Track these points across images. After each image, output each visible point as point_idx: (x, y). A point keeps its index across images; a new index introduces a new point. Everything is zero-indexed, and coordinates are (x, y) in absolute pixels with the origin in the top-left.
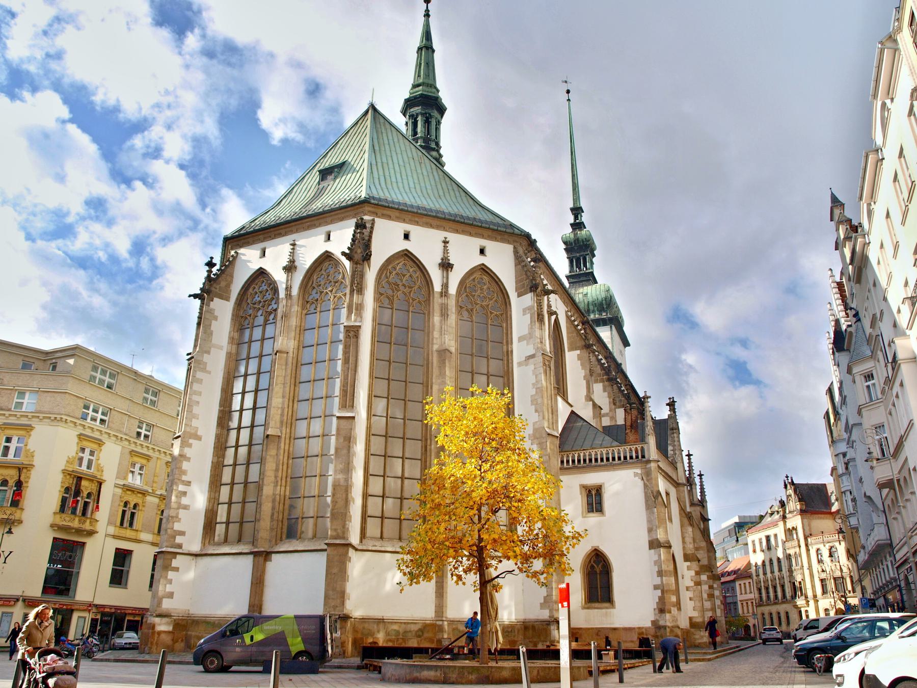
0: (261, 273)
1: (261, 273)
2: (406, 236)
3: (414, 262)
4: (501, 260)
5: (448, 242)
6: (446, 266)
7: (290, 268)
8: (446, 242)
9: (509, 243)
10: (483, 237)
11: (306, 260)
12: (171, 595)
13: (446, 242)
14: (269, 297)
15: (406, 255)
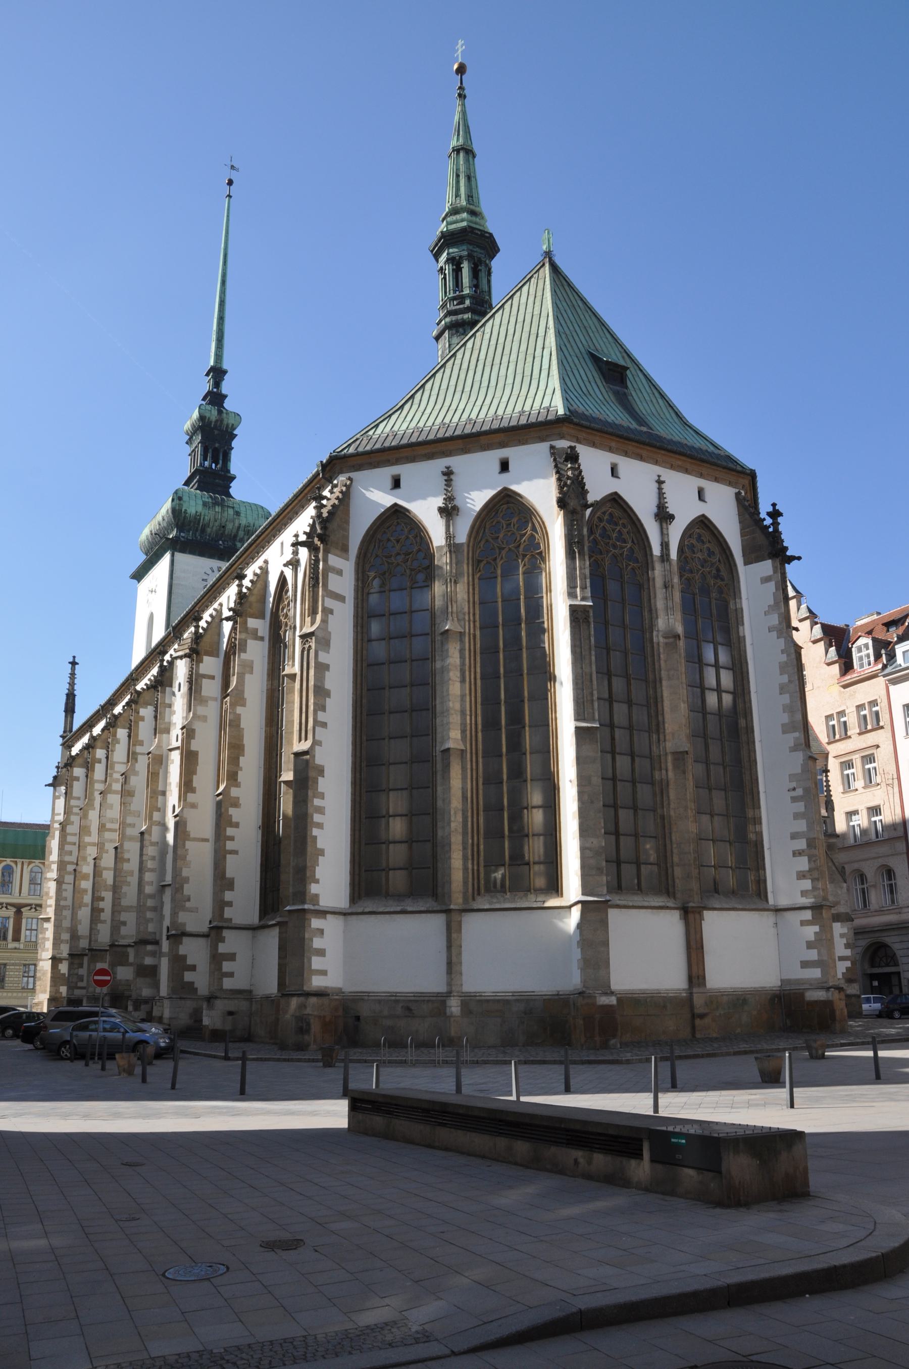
0: (397, 513)
1: (397, 513)
2: (614, 471)
3: (625, 511)
4: (721, 506)
5: (663, 482)
6: (664, 516)
7: (449, 512)
8: (660, 482)
9: (730, 484)
10: (701, 476)
11: (477, 499)
12: (324, 973)
13: (660, 482)
14: (415, 549)
15: (614, 500)
